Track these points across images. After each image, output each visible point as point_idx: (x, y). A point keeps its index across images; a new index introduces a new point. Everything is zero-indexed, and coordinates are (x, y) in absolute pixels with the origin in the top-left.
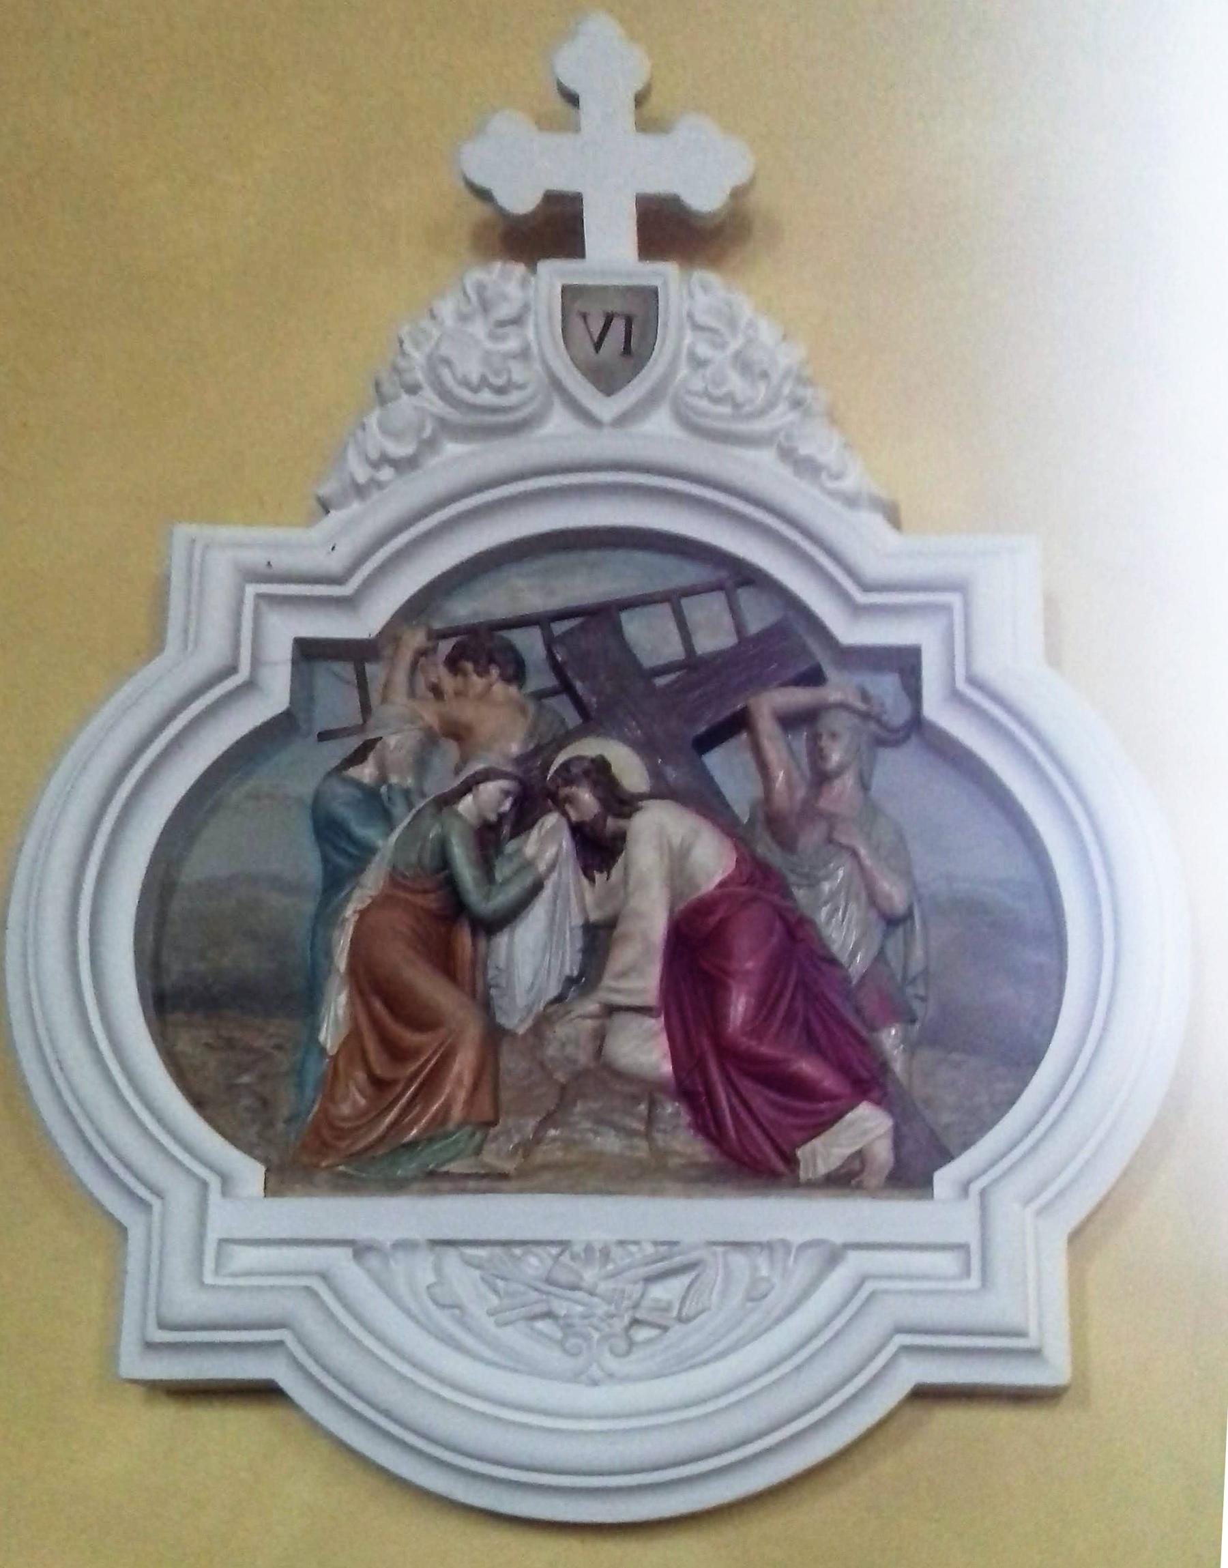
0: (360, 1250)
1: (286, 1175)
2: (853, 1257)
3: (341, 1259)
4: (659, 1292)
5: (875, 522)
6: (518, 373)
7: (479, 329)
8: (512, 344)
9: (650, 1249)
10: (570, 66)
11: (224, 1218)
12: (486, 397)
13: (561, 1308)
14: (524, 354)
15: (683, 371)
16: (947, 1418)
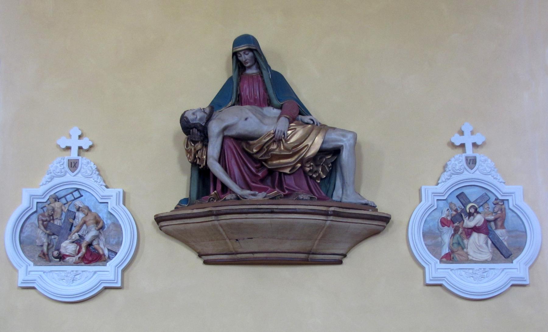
0: (44, 272)
1: (35, 264)
2: (99, 273)
3: (42, 273)
4: (76, 277)
5: (104, 187)
6: (63, 170)
7: (58, 165)
8: (62, 167)
9: (75, 272)
10: (71, 132)
11: (30, 269)
12: (59, 174)
13: (65, 278)
14: (64, 168)
15: (82, 169)
16: (107, 291)
